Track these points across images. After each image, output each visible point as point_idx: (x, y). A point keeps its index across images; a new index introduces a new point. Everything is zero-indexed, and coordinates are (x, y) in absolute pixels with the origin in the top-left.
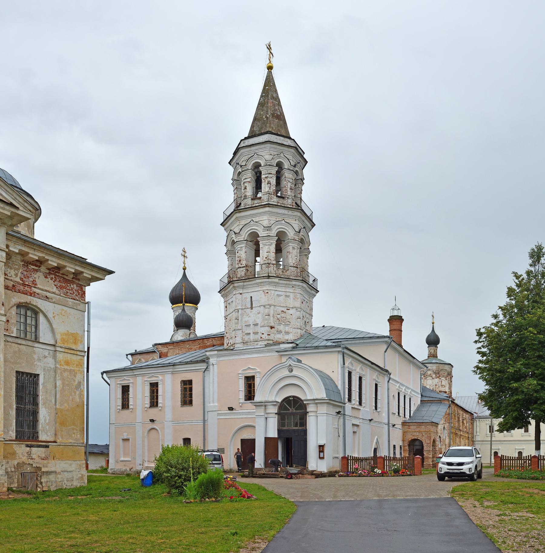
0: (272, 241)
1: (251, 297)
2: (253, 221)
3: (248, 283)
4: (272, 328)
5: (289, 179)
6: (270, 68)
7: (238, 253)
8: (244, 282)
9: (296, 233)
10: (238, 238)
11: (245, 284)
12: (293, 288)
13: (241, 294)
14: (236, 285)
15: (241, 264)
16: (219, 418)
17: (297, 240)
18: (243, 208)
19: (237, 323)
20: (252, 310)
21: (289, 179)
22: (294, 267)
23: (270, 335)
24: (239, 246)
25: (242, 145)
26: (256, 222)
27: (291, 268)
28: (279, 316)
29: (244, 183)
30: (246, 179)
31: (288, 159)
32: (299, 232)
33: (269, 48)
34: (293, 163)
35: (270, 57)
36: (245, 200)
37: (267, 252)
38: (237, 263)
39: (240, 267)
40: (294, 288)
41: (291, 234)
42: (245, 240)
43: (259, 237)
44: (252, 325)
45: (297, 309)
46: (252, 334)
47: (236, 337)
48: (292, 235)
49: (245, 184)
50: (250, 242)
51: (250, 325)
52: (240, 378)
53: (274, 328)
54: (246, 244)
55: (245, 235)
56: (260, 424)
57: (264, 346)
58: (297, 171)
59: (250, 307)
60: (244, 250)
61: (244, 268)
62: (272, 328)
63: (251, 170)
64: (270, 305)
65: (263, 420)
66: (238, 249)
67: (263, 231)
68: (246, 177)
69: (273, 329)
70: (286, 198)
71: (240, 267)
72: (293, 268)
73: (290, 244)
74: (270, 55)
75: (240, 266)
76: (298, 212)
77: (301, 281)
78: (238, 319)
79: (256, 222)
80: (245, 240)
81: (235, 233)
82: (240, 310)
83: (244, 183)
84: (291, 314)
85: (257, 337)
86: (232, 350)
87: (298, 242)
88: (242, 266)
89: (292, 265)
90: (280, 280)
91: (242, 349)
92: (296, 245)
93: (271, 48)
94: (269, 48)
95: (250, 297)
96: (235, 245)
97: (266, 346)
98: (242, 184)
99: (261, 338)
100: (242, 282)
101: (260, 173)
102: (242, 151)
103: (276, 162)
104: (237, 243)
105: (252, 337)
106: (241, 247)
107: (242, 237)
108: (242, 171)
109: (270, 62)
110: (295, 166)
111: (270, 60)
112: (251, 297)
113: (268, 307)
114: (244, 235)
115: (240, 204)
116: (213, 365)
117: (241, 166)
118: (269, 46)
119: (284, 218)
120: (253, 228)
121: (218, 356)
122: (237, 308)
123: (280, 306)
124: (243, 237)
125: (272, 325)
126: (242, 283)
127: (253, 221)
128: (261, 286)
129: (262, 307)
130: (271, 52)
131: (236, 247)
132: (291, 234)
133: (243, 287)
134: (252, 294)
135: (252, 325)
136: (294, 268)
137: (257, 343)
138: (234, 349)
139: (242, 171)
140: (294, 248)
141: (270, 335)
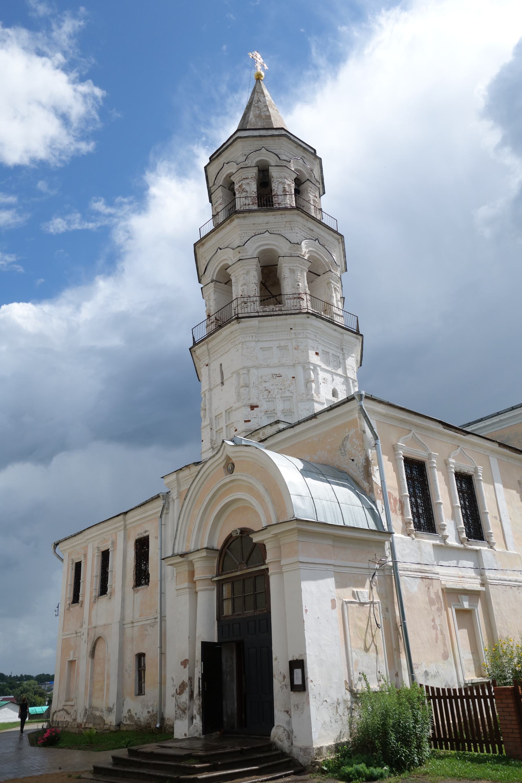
1: (221, 365)
2: (220, 249)
4: (253, 407)
5: (280, 180)
11: (210, 346)
13: (207, 365)
21: (280, 180)
23: (249, 421)
28: (267, 385)
47: (202, 441)
50: (226, 284)
53: (257, 407)
62: (253, 407)
64: (248, 369)
69: (255, 409)
72: (292, 301)
76: (294, 214)
84: (293, 378)
95: (219, 365)
99: (236, 430)
112: (221, 365)
123: (268, 366)
125: (254, 402)
126: (206, 346)
127: (220, 249)
136: (295, 300)
141: (249, 421)
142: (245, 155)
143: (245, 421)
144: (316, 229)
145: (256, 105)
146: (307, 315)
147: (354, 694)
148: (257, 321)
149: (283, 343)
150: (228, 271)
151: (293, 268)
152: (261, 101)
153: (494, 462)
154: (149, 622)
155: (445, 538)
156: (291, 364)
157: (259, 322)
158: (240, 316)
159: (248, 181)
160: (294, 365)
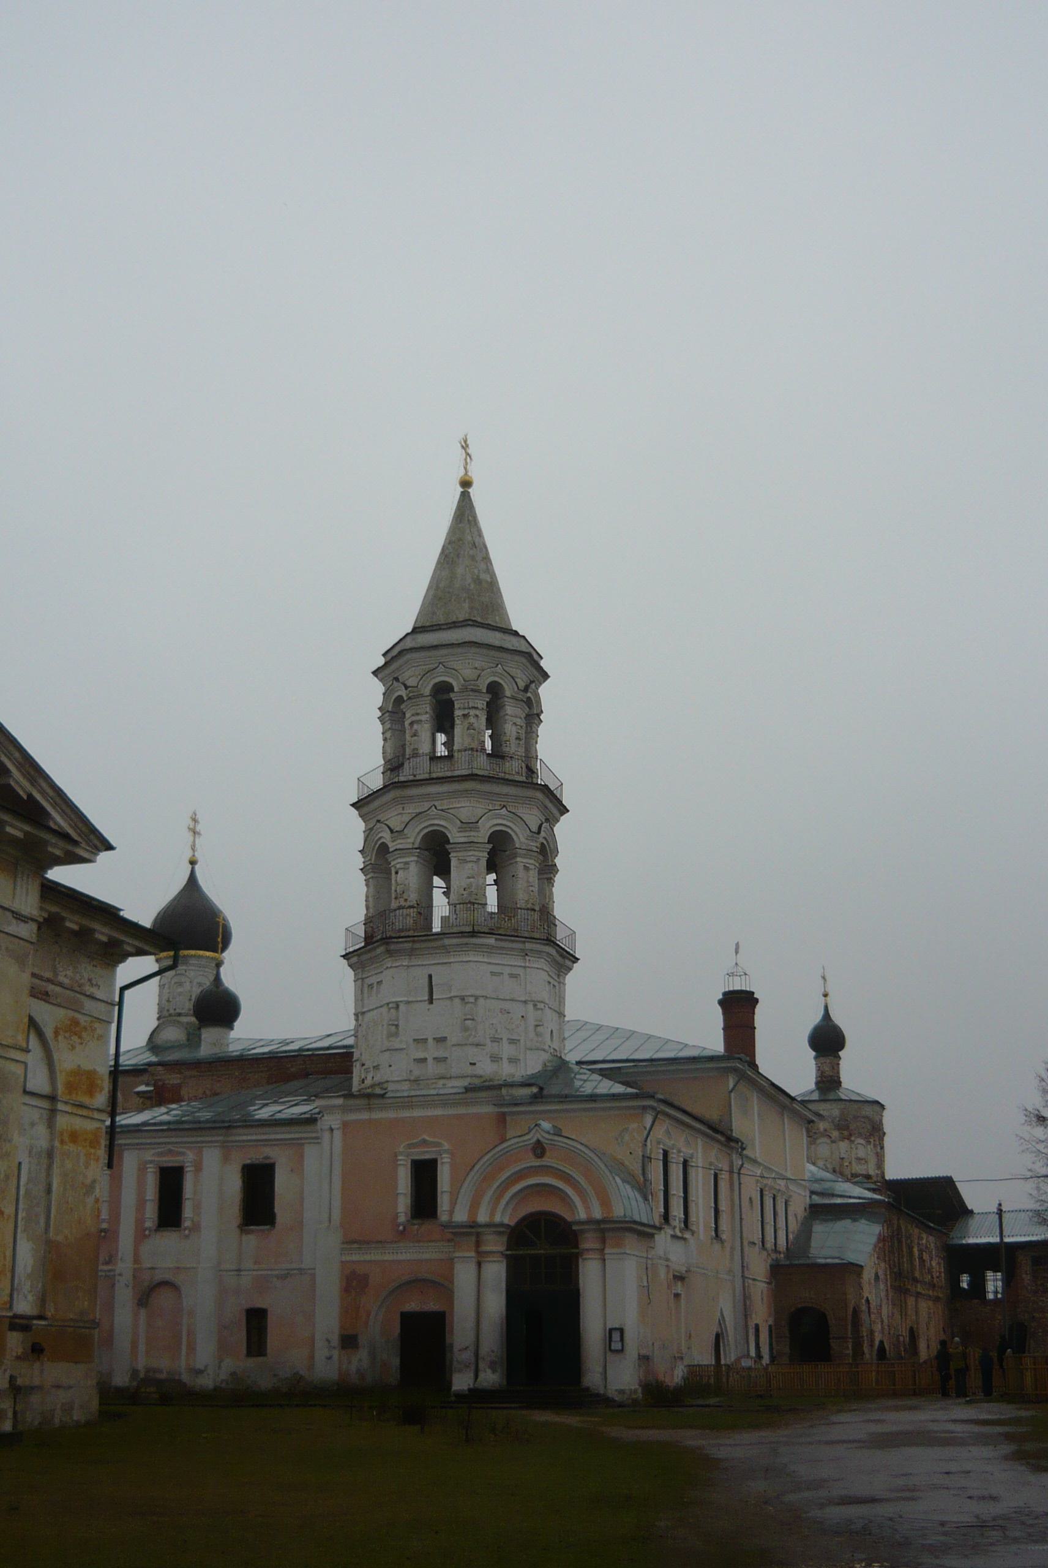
0: (481, 854)
1: (430, 976)
2: (436, 808)
3: (423, 945)
6: (466, 484)
7: (397, 873)
8: (414, 941)
9: (531, 834)
10: (399, 841)
11: (417, 945)
12: (527, 958)
14: (392, 947)
15: (406, 900)
16: (344, 1258)
17: (535, 849)
18: (411, 778)
19: (396, 1034)
20: (431, 1006)
22: (528, 909)
23: (474, 1064)
24: (399, 860)
25: (409, 643)
26: (442, 810)
27: (519, 910)
29: (412, 724)
30: (418, 714)
31: (512, 677)
32: (539, 833)
33: (465, 446)
34: (522, 685)
35: (466, 463)
36: (413, 761)
37: (469, 878)
38: (393, 896)
39: (403, 908)
40: (530, 958)
41: (521, 836)
42: (416, 849)
43: (448, 842)
44: (430, 1041)
45: (535, 1005)
46: (430, 1061)
48: (523, 839)
49: (415, 726)
51: (427, 1039)
52: (399, 1163)
54: (418, 856)
55: (416, 838)
56: (464, 1276)
57: (464, 1091)
58: (529, 698)
59: (426, 998)
60: (413, 869)
61: (412, 910)
63: (429, 698)
64: (477, 998)
65: (473, 1267)
66: (398, 866)
67: (459, 832)
68: (419, 711)
70: (509, 759)
71: (403, 908)
73: (518, 859)
74: (466, 459)
75: (403, 903)
77: (545, 942)
78: (397, 1026)
79: (442, 810)
80: (416, 849)
81: (392, 831)
82: (402, 1007)
83: (412, 724)
84: (523, 1017)
85: (440, 1069)
86: (382, 1096)
87: (536, 854)
88: (408, 904)
89: (523, 906)
90: (501, 940)
91: (406, 1094)
93: (467, 446)
94: (465, 446)
95: (427, 976)
96: (390, 857)
97: (468, 1090)
98: (407, 723)
100: (409, 942)
101: (450, 704)
102: (408, 656)
103: (487, 682)
104: (396, 853)
105: (432, 1068)
106: (406, 863)
107: (409, 840)
108: (409, 698)
109: (466, 474)
110: (526, 689)
111: (465, 469)
112: (430, 976)
113: (472, 1000)
114: (414, 836)
116: (332, 1130)
117: (406, 687)
118: (465, 442)
119: (505, 803)
120: (436, 822)
121: (345, 1109)
122: (394, 1000)
124: (411, 840)
126: (410, 945)
128: (455, 953)
129: (457, 1000)
130: (468, 454)
131: (394, 860)
132: (520, 838)
133: (412, 953)
134: (432, 970)
135: (430, 1041)
137: (442, 1082)
138: (387, 1096)
139: (409, 698)
140: (526, 868)
142: (476, 668)
143: (471, 1064)
144: (550, 805)
145: (471, 552)
146: (547, 942)
147: (639, 1356)
148: (494, 939)
149: (515, 971)
150: (448, 847)
151: (528, 865)
152: (477, 544)
153: (699, 1141)
154: (274, 1273)
155: (675, 1228)
156: (524, 999)
157: (496, 939)
158: (476, 929)
159: (478, 712)
160: (525, 1002)
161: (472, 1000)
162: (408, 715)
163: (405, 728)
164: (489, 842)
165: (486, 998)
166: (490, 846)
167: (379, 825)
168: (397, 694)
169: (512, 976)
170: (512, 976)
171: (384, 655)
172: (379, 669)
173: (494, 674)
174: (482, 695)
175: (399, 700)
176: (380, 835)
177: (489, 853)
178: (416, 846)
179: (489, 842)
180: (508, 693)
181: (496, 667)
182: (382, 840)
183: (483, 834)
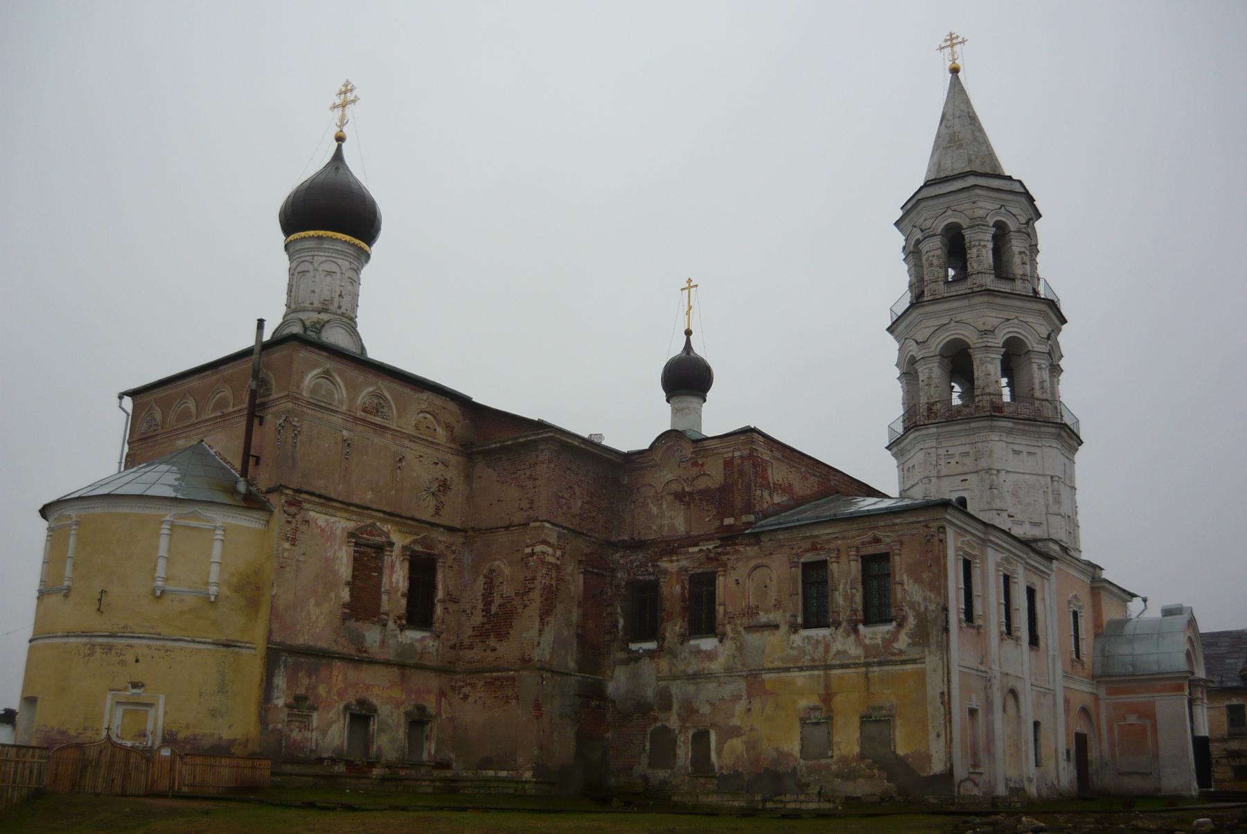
31: (1014, 215)
43: (970, 348)
90: (1018, 423)
92: (1045, 363)
115: (923, 292)
149: (1032, 450)
161: (995, 472)
162: (923, 253)
163: (923, 264)
164: (1003, 347)
165: (1007, 472)
166: (1004, 350)
167: (907, 340)
168: (916, 238)
169: (1029, 453)
170: (1029, 453)
171: (902, 208)
172: (897, 221)
173: (997, 214)
174: (990, 229)
175: (918, 242)
176: (909, 349)
177: (1002, 356)
178: (937, 354)
179: (1003, 347)
180: (1012, 229)
181: (1000, 208)
182: (911, 353)
183: (999, 340)
